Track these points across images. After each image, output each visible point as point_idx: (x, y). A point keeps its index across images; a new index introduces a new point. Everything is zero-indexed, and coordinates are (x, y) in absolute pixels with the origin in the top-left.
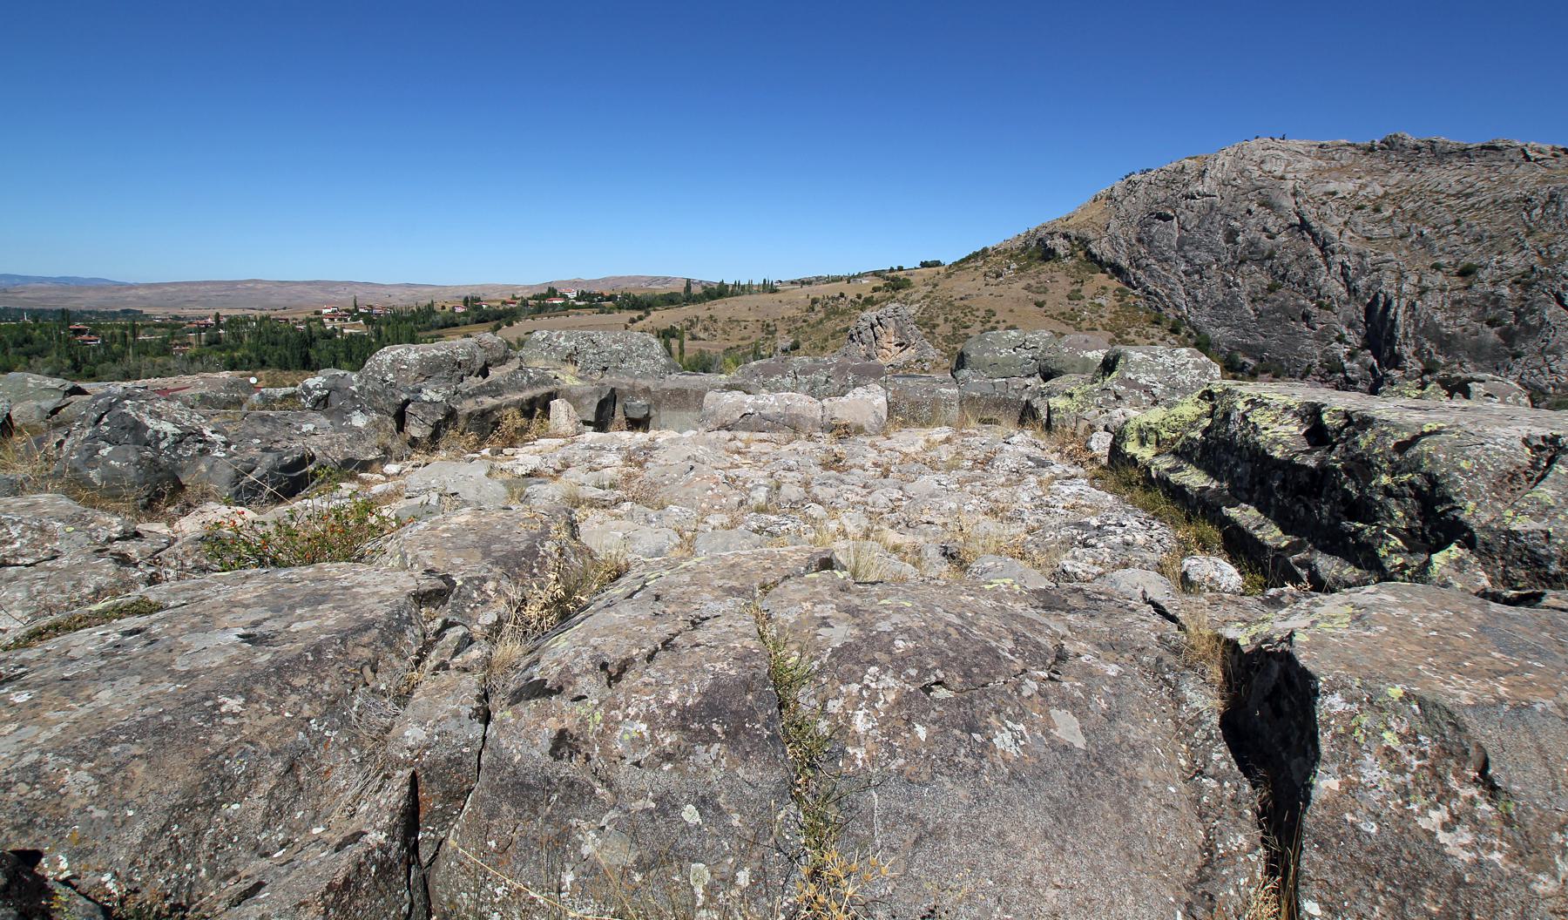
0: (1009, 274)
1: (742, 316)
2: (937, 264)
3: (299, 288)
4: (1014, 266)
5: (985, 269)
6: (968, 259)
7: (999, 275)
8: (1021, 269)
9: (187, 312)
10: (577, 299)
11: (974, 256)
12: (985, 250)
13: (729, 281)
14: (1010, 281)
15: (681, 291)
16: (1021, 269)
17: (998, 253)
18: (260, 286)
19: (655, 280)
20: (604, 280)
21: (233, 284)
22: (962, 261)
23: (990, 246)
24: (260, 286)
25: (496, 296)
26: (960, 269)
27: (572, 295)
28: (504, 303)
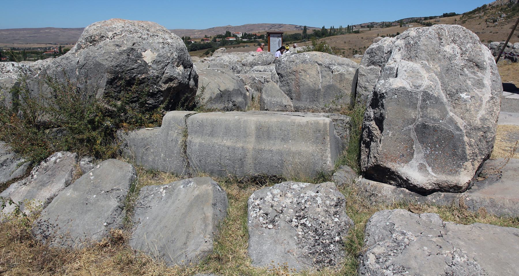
0: (502, 20)
1: (341, 46)
2: (453, 14)
3: (73, 32)
4: (504, 15)
5: (485, 18)
6: (474, 12)
7: (495, 21)
8: (508, 17)
9: (16, 46)
10: (243, 37)
11: (478, 10)
12: (484, 6)
13: (328, 27)
14: (502, 24)
15: (301, 32)
16: (508, 17)
17: (493, 7)
18: (52, 31)
19: (273, 25)
20: (244, 26)
21: (38, 30)
22: (470, 13)
23: (487, 4)
24: (52, 31)
25: (197, 35)
26: (470, 18)
27: (240, 35)
28: (203, 40)
